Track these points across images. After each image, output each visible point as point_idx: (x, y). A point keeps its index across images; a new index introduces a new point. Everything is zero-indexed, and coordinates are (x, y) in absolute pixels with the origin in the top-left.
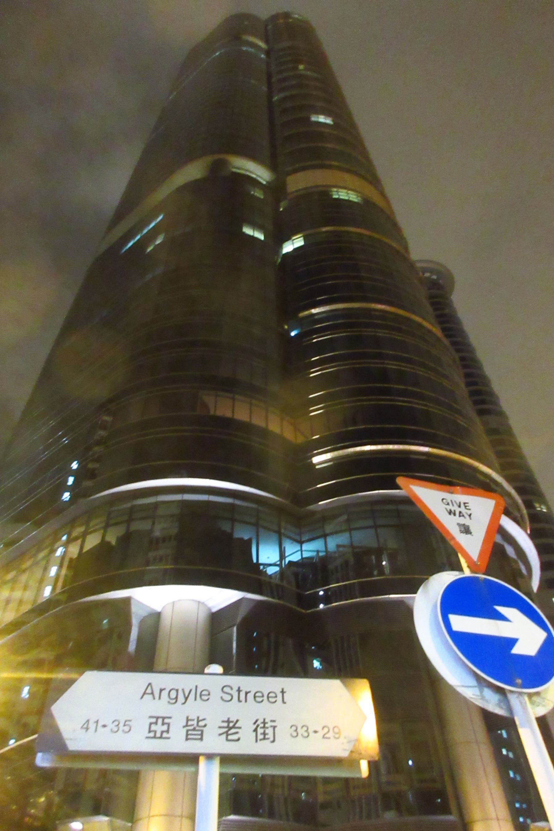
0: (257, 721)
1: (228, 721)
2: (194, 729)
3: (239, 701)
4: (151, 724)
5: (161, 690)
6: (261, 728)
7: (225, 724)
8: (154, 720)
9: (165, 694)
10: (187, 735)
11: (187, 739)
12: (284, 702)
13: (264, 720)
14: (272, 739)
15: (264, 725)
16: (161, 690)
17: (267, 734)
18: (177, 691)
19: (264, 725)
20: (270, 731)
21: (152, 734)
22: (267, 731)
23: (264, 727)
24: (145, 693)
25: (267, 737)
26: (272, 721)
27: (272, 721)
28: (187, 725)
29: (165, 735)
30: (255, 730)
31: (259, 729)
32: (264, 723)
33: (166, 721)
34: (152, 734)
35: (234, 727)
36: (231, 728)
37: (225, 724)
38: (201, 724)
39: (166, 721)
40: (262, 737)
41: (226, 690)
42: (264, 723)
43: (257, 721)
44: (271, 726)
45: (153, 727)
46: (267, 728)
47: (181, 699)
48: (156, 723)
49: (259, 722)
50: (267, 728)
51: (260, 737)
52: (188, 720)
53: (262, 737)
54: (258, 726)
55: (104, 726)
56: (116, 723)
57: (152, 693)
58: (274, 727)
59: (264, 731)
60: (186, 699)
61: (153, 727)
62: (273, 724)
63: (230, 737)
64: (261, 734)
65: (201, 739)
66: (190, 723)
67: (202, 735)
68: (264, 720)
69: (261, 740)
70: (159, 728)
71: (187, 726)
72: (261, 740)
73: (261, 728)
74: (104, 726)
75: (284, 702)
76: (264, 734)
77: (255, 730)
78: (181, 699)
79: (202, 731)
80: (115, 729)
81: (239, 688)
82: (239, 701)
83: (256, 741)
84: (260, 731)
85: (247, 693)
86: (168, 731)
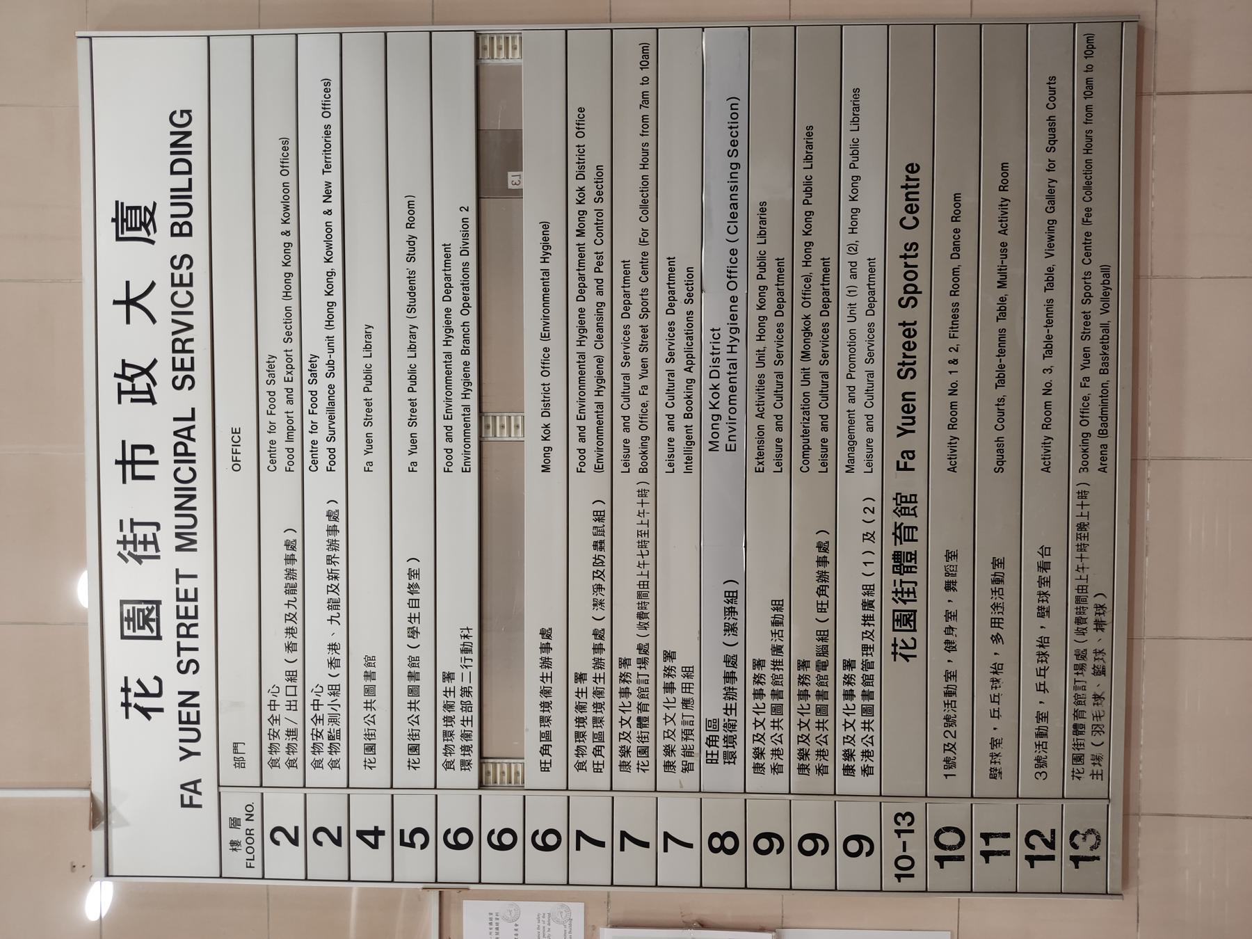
0: (120, 554)
6: (135, 550)
17: (145, 536)
25: (150, 538)
26: (121, 530)
27: (121, 530)
30: (139, 559)
40: (151, 548)
43: (120, 554)
44: (132, 531)
46: (135, 536)
49: (125, 553)
50: (135, 536)
53: (151, 548)
54: (130, 554)
64: (145, 549)
68: (119, 542)
69: (157, 550)
72: (157, 550)
73: (135, 550)
83: (158, 557)
84: (140, 551)
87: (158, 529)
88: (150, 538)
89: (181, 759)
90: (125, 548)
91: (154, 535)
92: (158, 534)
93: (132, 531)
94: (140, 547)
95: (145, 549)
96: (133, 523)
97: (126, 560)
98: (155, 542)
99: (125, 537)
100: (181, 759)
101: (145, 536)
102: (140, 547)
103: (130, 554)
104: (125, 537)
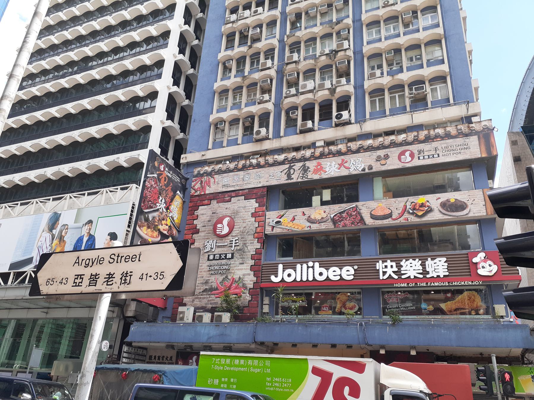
1: (110, 274)
2: (93, 280)
3: (117, 262)
4: (75, 279)
5: (83, 260)
7: (108, 276)
8: (77, 277)
9: (84, 261)
10: (90, 283)
11: (89, 285)
12: (139, 261)
16: (83, 260)
18: (89, 260)
20: (128, 278)
21: (75, 284)
22: (127, 278)
24: (75, 263)
28: (91, 278)
29: (80, 284)
30: (121, 279)
33: (82, 277)
34: (75, 284)
35: (112, 277)
36: (109, 278)
37: (108, 276)
38: (97, 277)
39: (82, 277)
41: (113, 256)
42: (127, 273)
45: (76, 281)
47: (91, 264)
48: (77, 278)
52: (92, 275)
55: (150, 276)
56: (156, 274)
57: (78, 263)
58: (131, 276)
60: (93, 263)
61: (76, 281)
62: (131, 274)
63: (109, 283)
65: (95, 286)
66: (92, 277)
67: (96, 283)
70: (78, 281)
71: (91, 278)
74: (150, 276)
75: (139, 261)
76: (125, 280)
77: (121, 279)
78: (91, 264)
79: (96, 281)
80: (156, 278)
82: (117, 262)
84: (123, 278)
85: (122, 257)
86: (81, 283)
96: (131, 276)
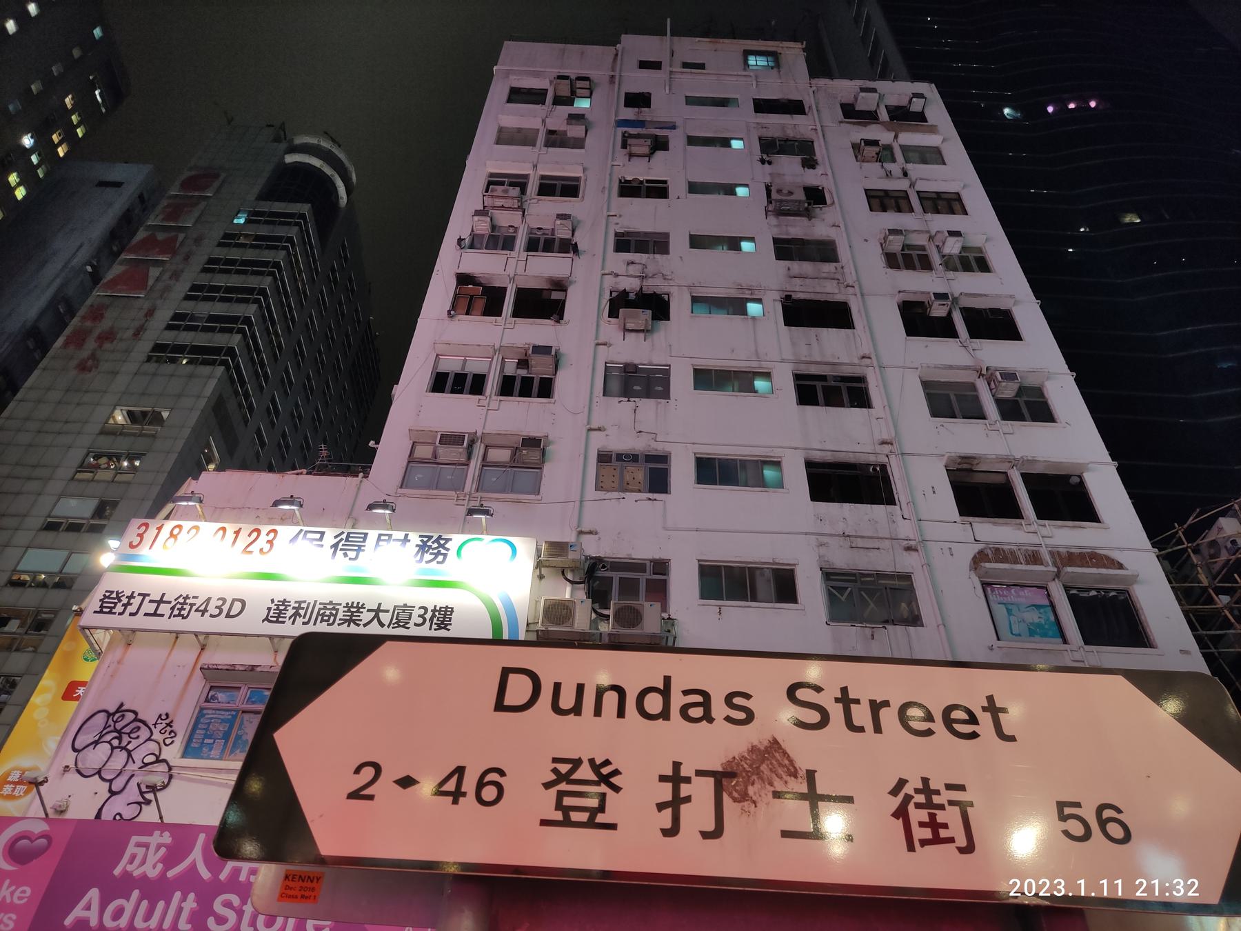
6: (918, 806)
13: (925, 781)
14: (962, 841)
15: (929, 799)
17: (945, 826)
19: (929, 799)
20: (950, 816)
22: (941, 817)
23: (929, 805)
25: (943, 833)
26: (949, 787)
27: (949, 787)
30: (901, 813)
31: (911, 807)
32: (926, 788)
40: (927, 833)
43: (902, 783)
44: (951, 803)
46: (942, 807)
49: (909, 789)
50: (942, 807)
51: (921, 833)
53: (927, 833)
54: (908, 798)
59: (932, 817)
64: (922, 824)
69: (924, 843)
72: (924, 843)
73: (918, 806)
76: (933, 824)
81: (844, 690)
83: (911, 847)
87: (962, 850)
88: (943, 833)
89: (544, 823)
90: (917, 791)
91: (951, 840)
92: (951, 847)
93: (951, 803)
94: (923, 815)
95: (922, 824)
97: (894, 792)
98: (936, 840)
99: (937, 792)
100: (544, 823)
101: (945, 826)
102: (923, 815)
103: (908, 798)
104: (937, 792)
